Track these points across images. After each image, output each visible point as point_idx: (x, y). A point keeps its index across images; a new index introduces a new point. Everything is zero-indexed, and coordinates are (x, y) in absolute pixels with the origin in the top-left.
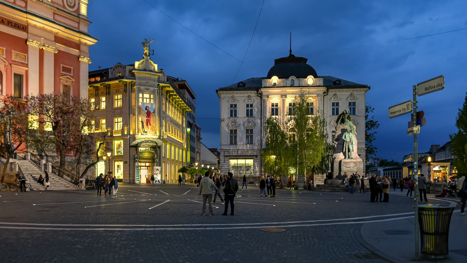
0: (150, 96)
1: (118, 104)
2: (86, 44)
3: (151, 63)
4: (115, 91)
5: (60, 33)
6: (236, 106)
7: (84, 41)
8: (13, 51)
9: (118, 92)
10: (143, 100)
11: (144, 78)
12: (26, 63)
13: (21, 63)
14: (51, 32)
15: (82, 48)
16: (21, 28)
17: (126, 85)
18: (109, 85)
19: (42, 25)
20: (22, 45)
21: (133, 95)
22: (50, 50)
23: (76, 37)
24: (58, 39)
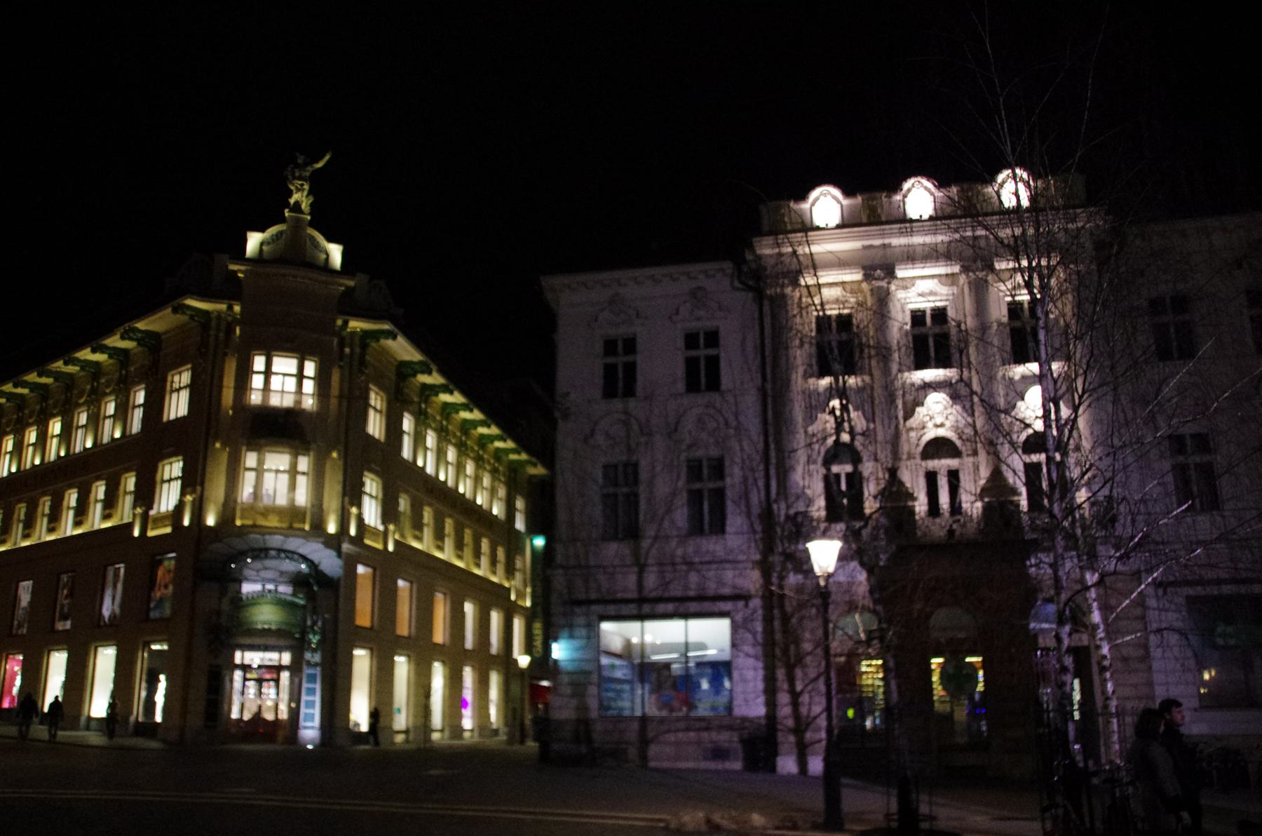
0: (301, 368)
1: (178, 406)
6: (630, 345)
10: (267, 382)
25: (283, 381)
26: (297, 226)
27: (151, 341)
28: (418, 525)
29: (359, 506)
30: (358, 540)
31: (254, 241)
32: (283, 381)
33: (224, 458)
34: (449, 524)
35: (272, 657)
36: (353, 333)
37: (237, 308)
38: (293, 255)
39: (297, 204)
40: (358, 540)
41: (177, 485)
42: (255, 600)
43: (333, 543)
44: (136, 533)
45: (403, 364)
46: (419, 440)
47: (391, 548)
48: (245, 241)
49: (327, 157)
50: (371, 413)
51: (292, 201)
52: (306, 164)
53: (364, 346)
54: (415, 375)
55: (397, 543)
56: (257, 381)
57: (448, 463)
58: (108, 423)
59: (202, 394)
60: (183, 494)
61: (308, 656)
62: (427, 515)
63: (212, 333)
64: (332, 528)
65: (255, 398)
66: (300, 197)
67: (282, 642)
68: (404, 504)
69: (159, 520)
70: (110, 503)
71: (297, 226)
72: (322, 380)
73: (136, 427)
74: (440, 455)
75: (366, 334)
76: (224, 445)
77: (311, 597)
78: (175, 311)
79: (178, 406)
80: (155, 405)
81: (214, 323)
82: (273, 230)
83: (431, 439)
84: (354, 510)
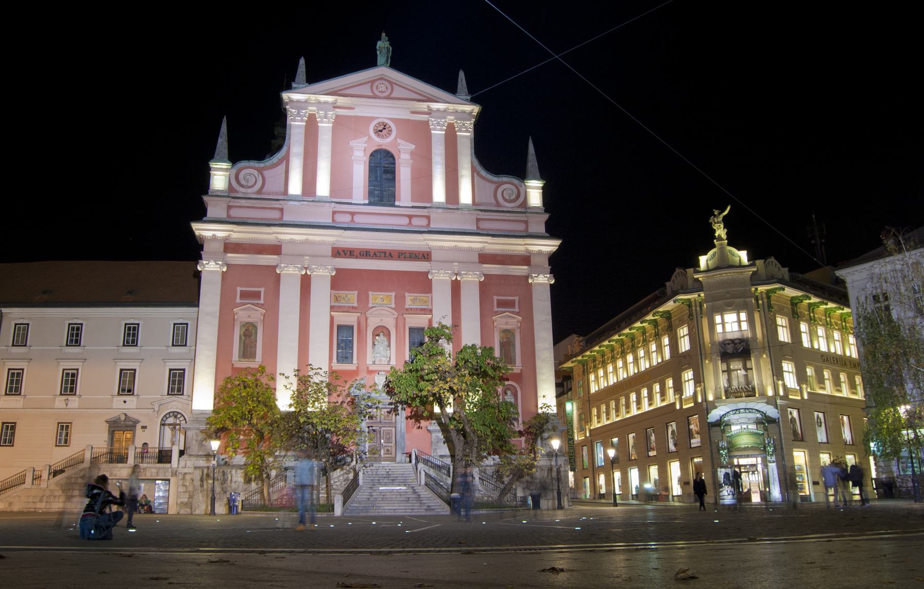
2: (540, 253)
3: (730, 251)
4: (677, 322)
5: (488, 246)
7: (536, 248)
8: (407, 294)
9: (681, 323)
10: (724, 327)
11: (722, 284)
12: (430, 307)
13: (421, 309)
14: (470, 250)
15: (533, 261)
16: (420, 256)
17: (690, 306)
18: (668, 312)
19: (453, 244)
20: (422, 283)
21: (705, 322)
22: (471, 279)
23: (518, 246)
24: (485, 258)
25: (731, 324)
26: (722, 249)
27: (668, 315)
28: (821, 380)
29: (783, 380)
30: (785, 397)
31: (703, 260)
32: (731, 324)
33: (711, 367)
34: (843, 377)
35: (751, 461)
36: (762, 292)
37: (702, 295)
38: (724, 264)
39: (719, 236)
40: (785, 397)
41: (692, 383)
42: (738, 435)
43: (771, 401)
44: (678, 407)
45: (793, 298)
46: (812, 334)
47: (806, 397)
48: (698, 261)
49: (729, 208)
50: (780, 329)
51: (717, 235)
52: (720, 214)
53: (769, 298)
54: (802, 301)
55: (809, 393)
56: (719, 329)
57: (835, 340)
58: (654, 355)
59: (695, 337)
60: (695, 387)
61: (769, 458)
62: (827, 374)
63: (694, 308)
64: (770, 393)
65: (719, 338)
66: (721, 231)
67: (756, 453)
68: (810, 371)
69: (687, 400)
70: (663, 393)
71: (722, 249)
72: (751, 321)
73: (667, 356)
74: (829, 338)
75: (768, 291)
76: (711, 361)
77: (766, 429)
78: (674, 302)
79: (685, 345)
80: (674, 345)
81: (693, 304)
82: (711, 253)
83: (821, 331)
84: (780, 382)
